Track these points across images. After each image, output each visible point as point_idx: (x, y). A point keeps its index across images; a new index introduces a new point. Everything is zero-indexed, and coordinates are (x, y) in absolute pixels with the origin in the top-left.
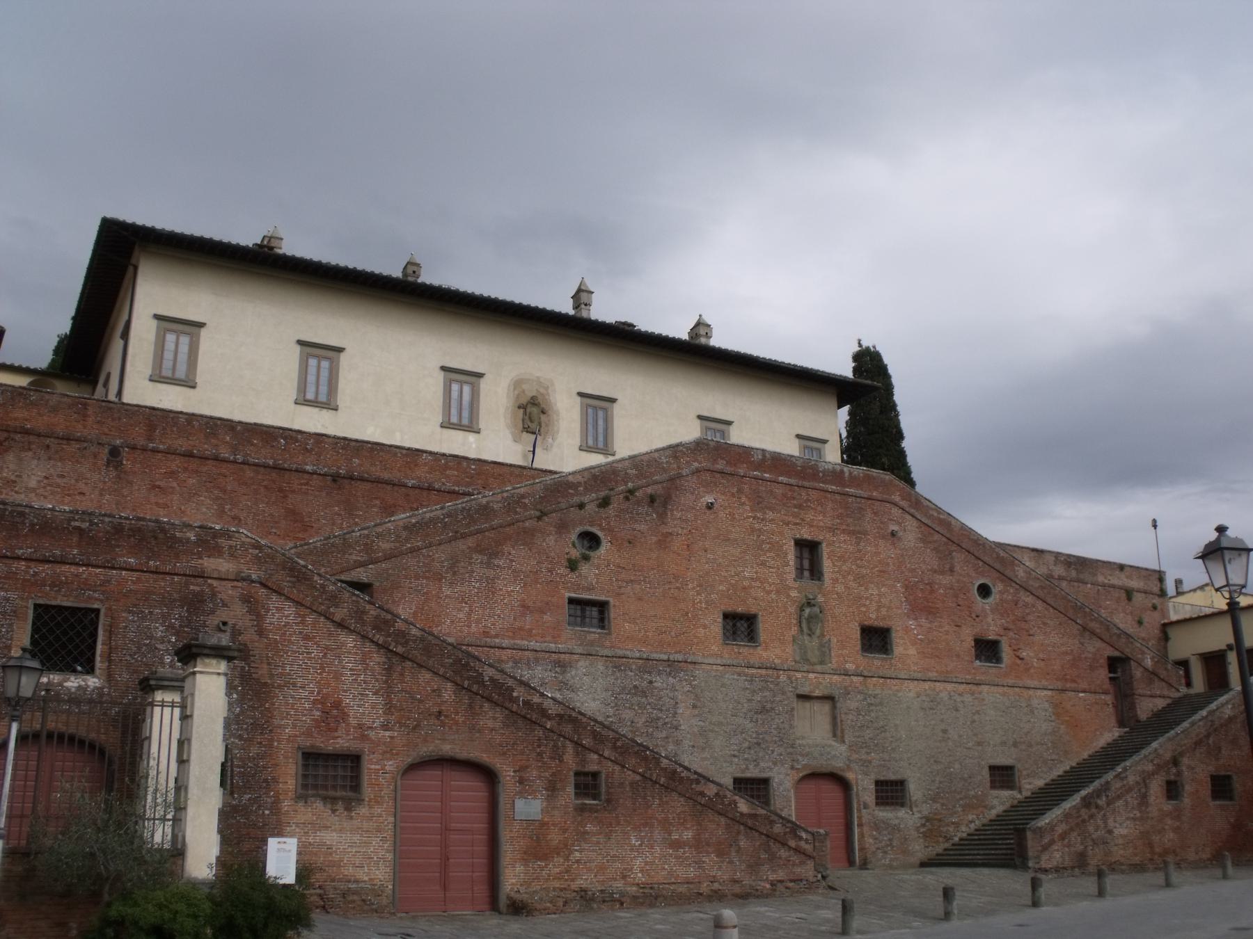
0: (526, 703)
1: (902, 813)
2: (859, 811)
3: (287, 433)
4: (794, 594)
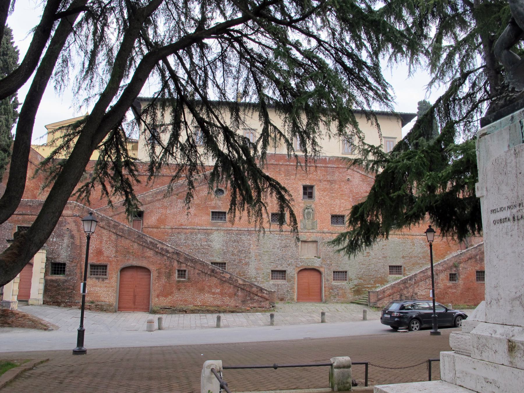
0: (162, 249)
1: (344, 283)
2: (325, 282)
4: (302, 205)
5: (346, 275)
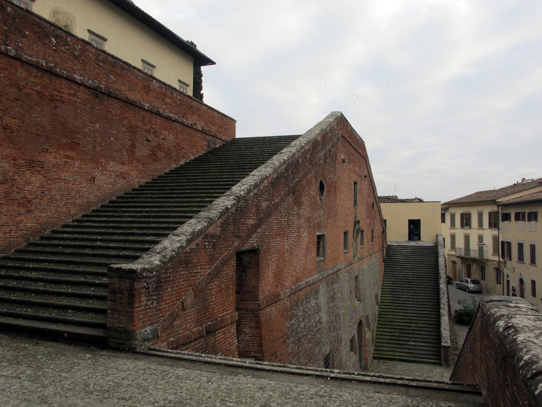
3: (58, 32)
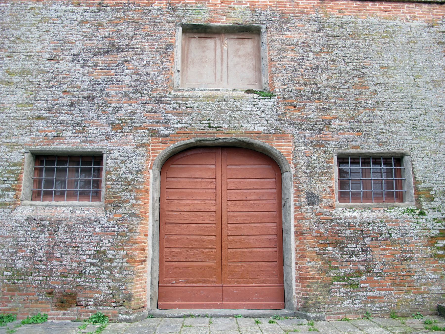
2: (298, 208)
5: (399, 173)
